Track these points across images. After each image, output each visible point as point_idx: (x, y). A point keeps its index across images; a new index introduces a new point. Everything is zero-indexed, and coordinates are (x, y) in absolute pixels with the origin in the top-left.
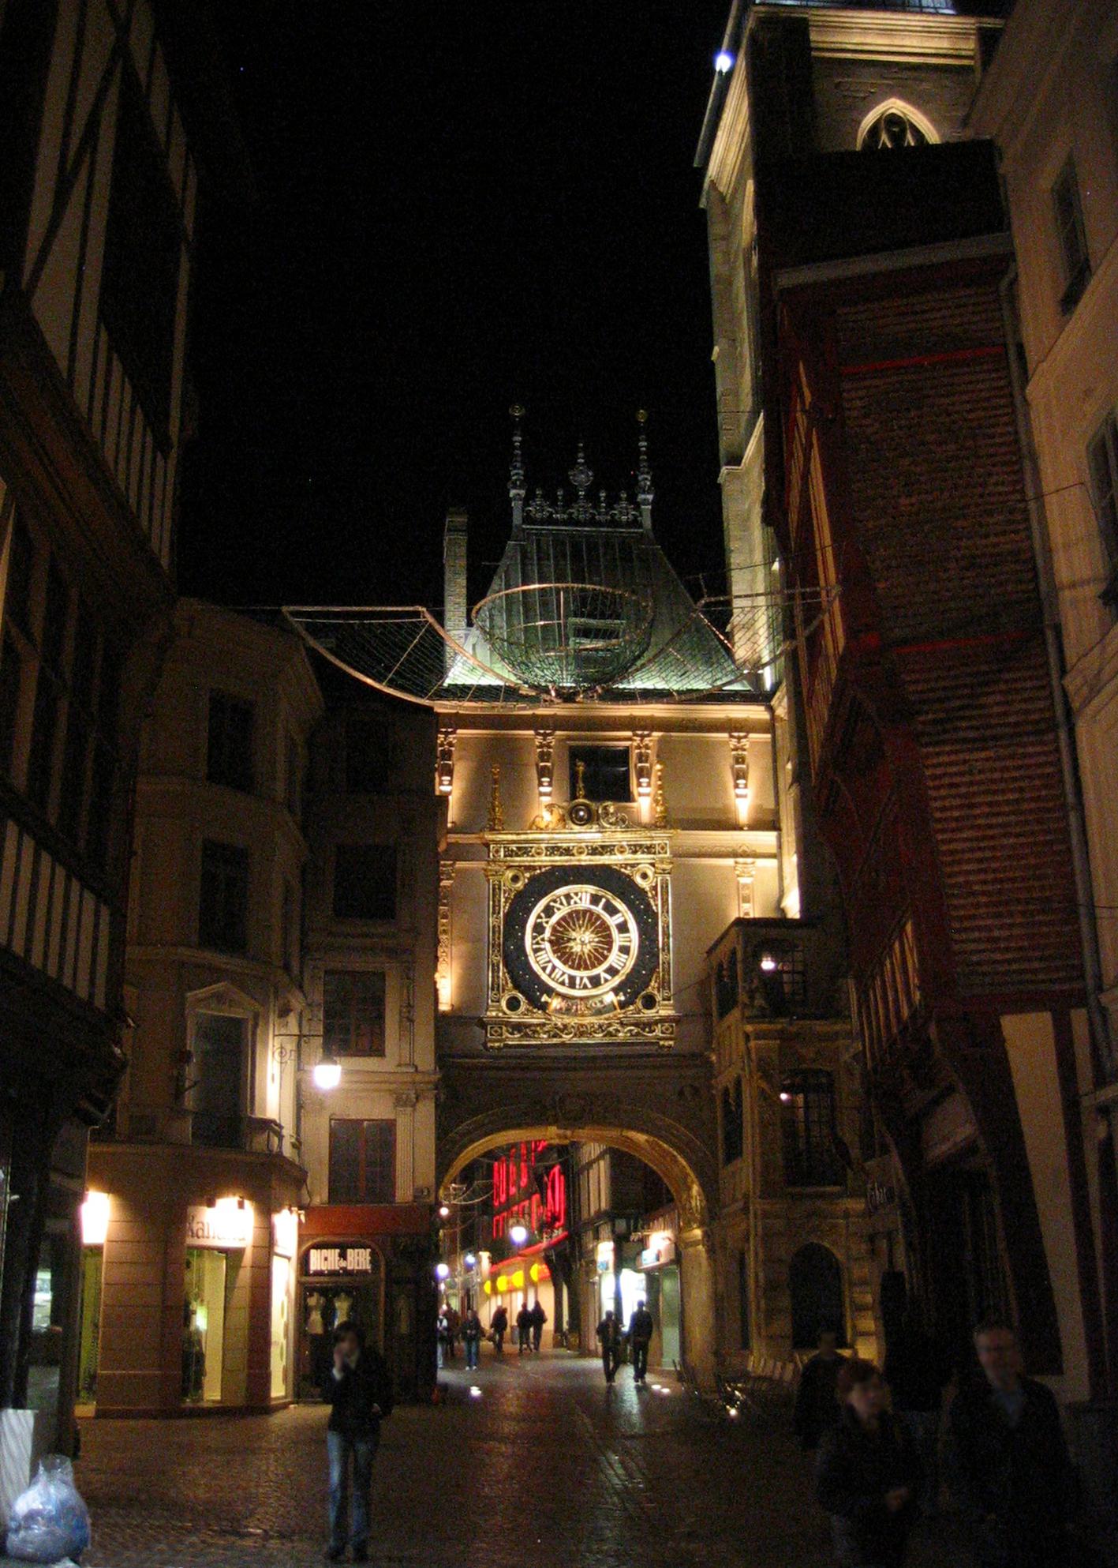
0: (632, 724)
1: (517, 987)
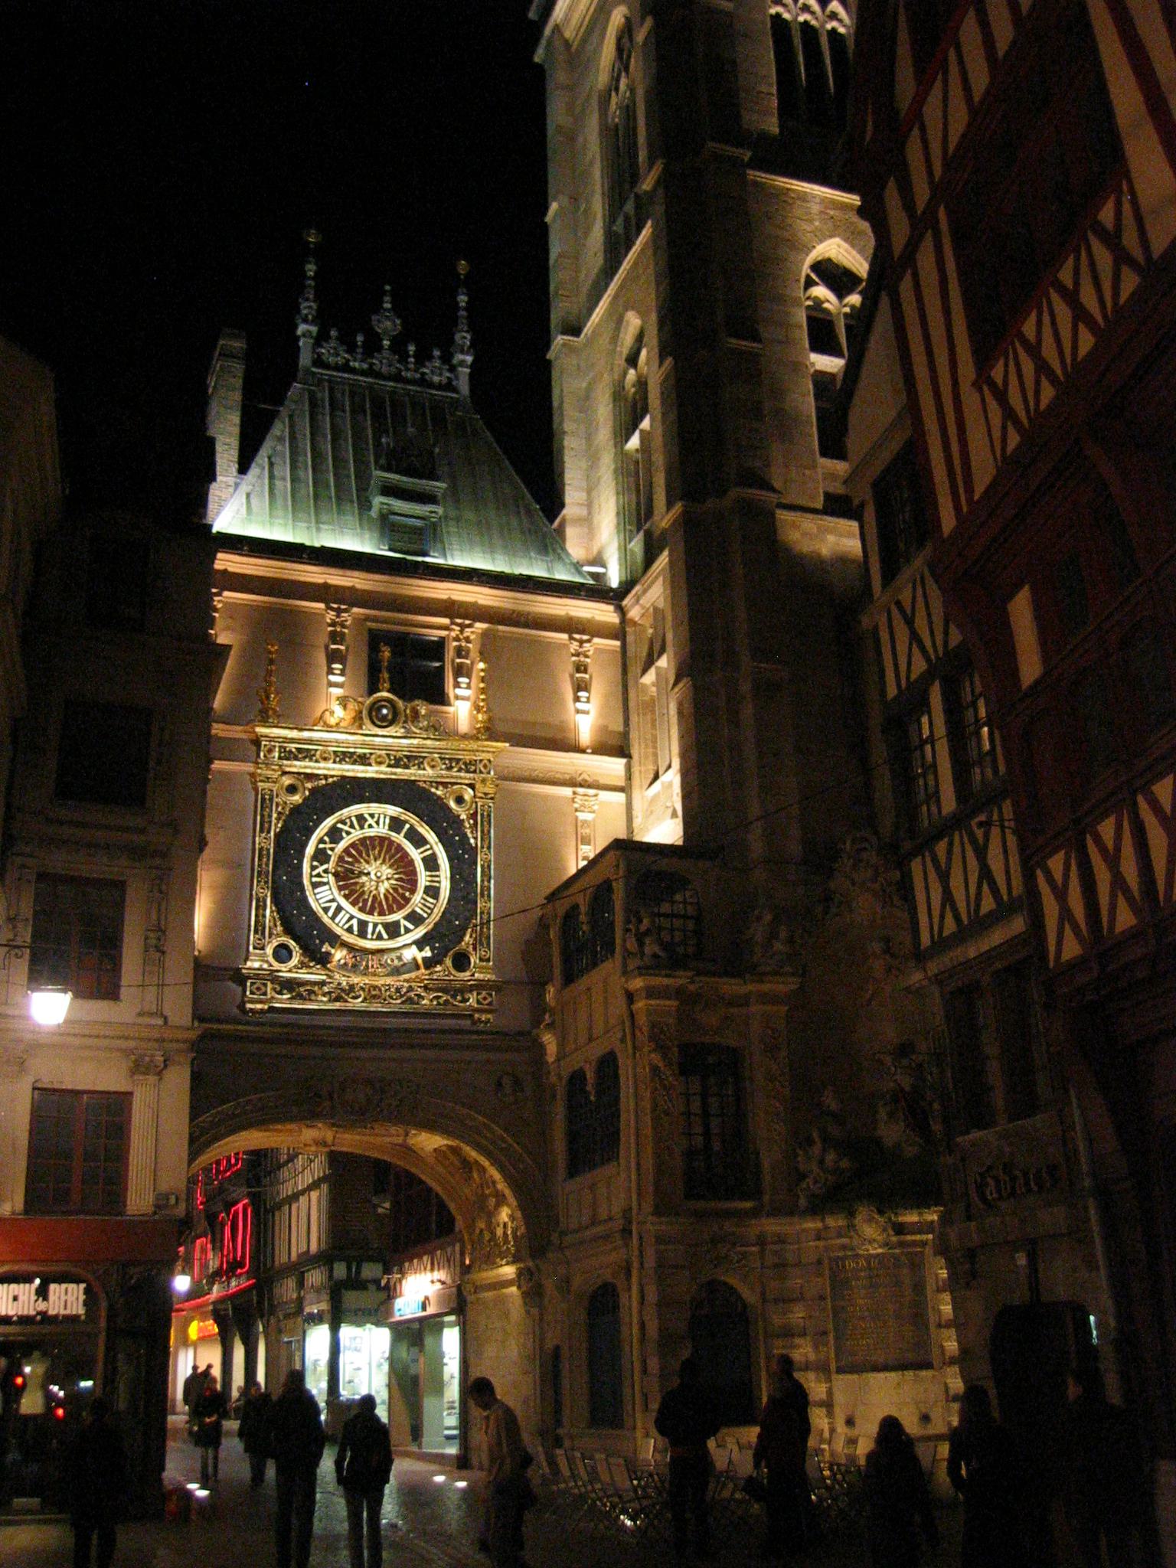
0: (449, 609)
1: (289, 931)
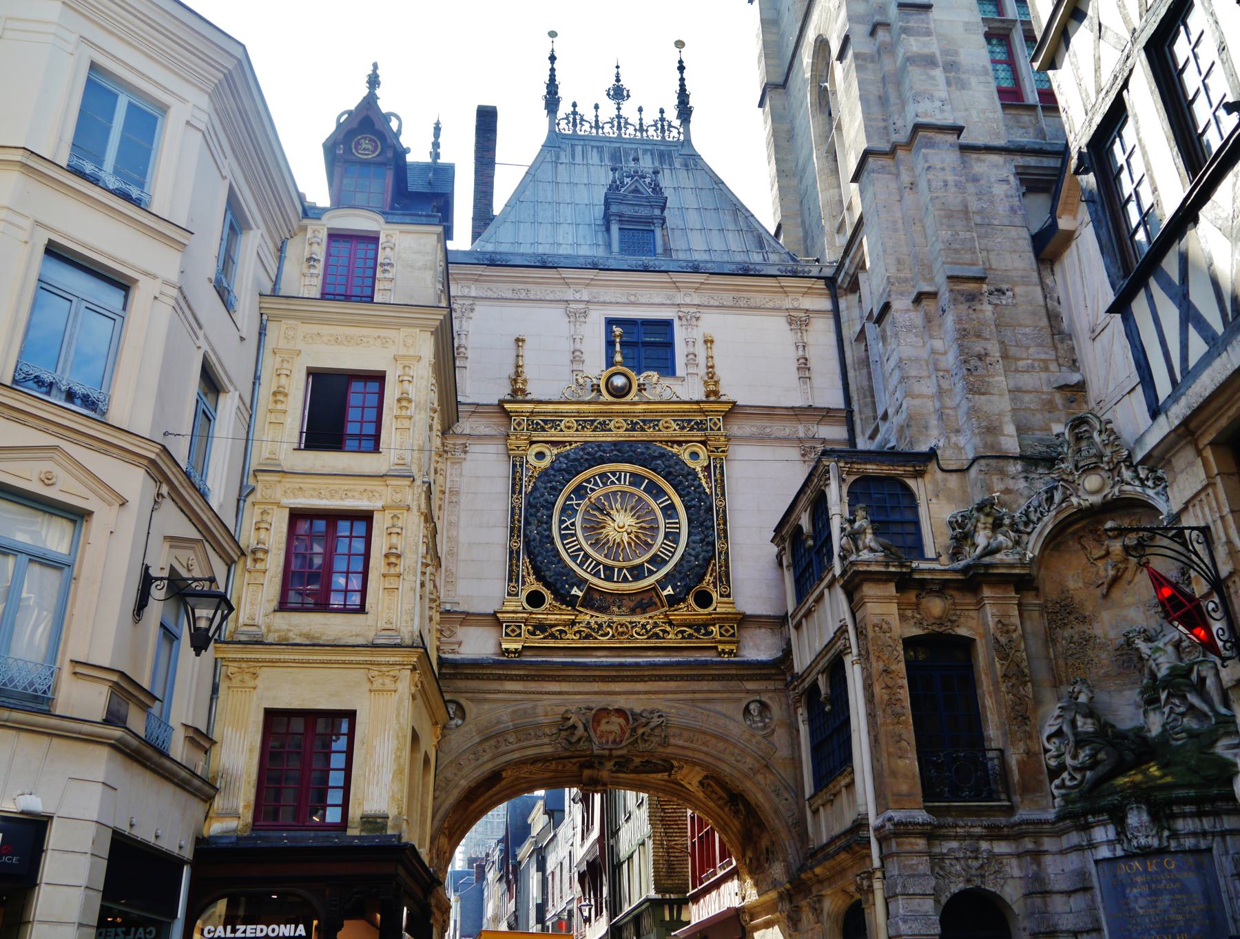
1: (540, 578)
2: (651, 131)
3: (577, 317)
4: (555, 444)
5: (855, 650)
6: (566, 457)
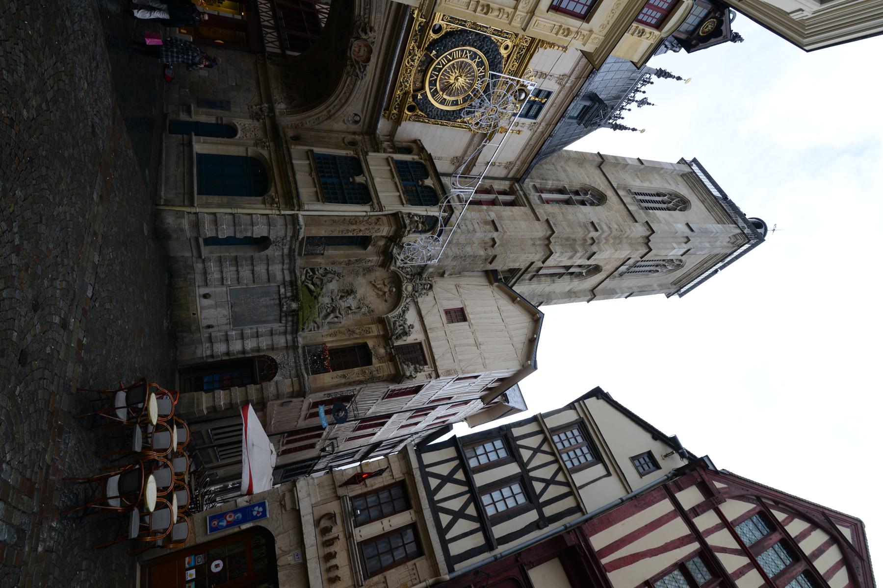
1: (447, 33)
2: (618, 112)
3: (561, 79)
4: (509, 56)
5: (372, 214)
6: (500, 63)
